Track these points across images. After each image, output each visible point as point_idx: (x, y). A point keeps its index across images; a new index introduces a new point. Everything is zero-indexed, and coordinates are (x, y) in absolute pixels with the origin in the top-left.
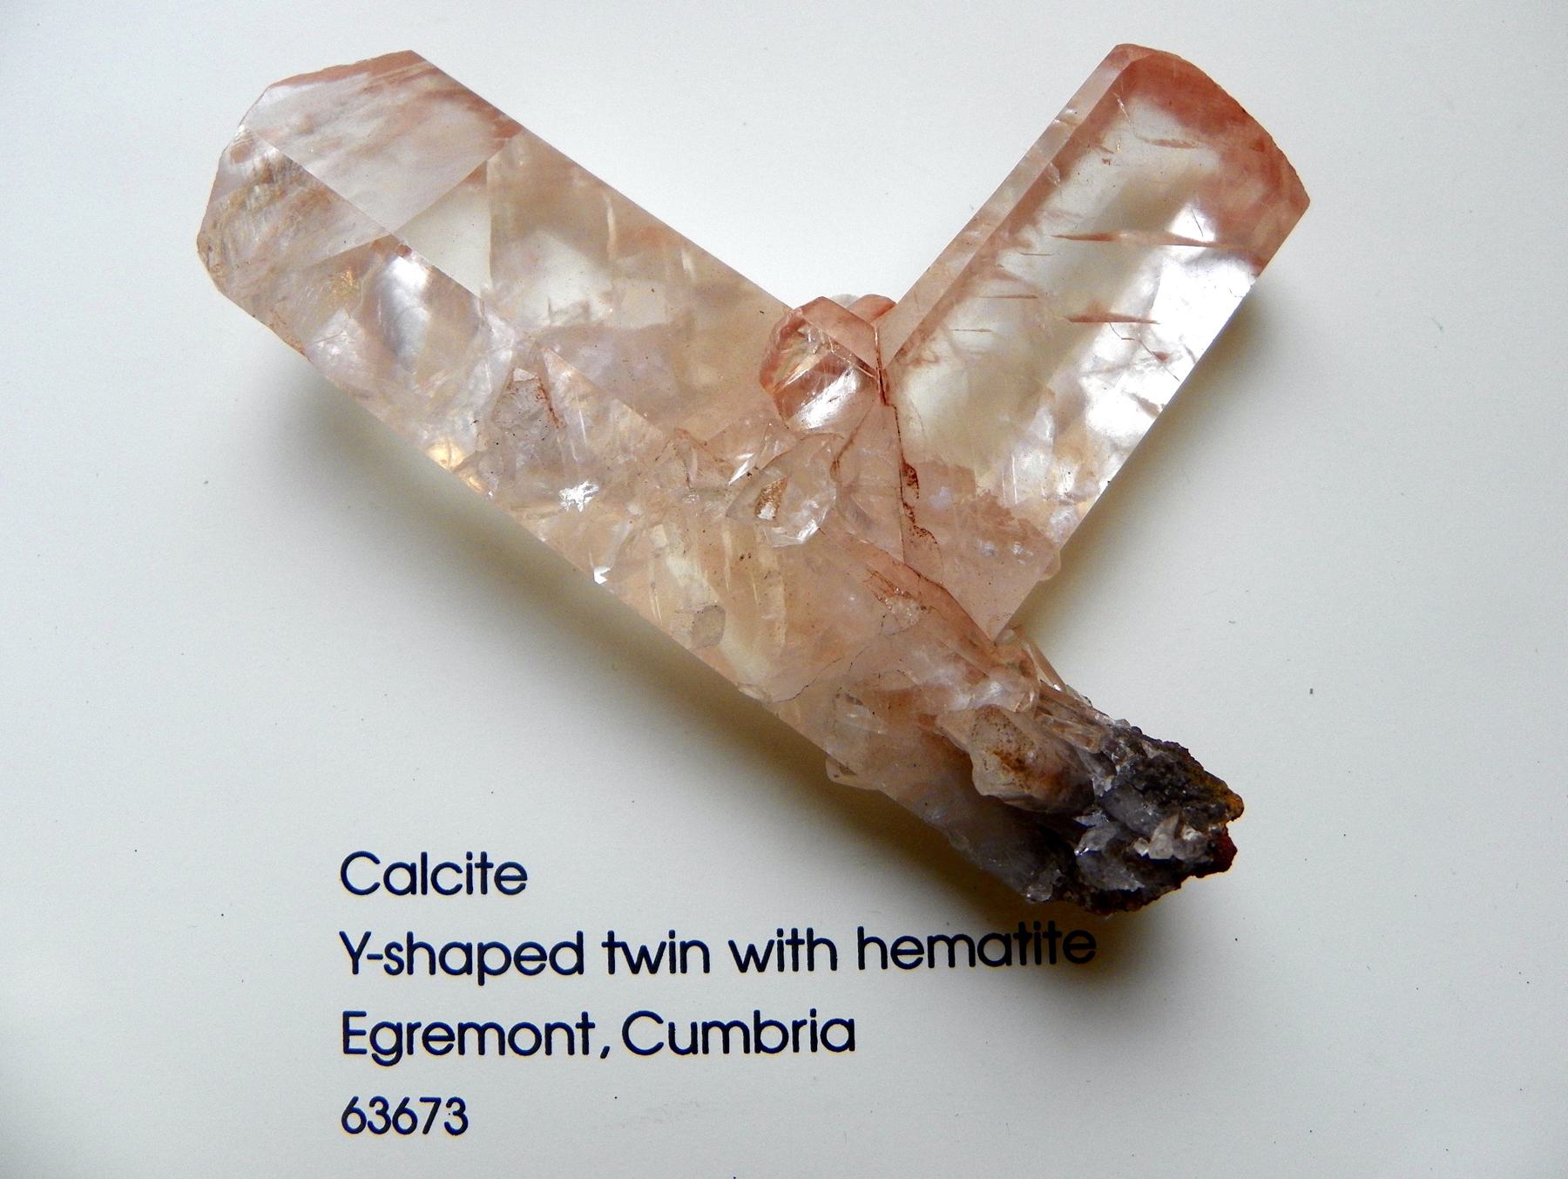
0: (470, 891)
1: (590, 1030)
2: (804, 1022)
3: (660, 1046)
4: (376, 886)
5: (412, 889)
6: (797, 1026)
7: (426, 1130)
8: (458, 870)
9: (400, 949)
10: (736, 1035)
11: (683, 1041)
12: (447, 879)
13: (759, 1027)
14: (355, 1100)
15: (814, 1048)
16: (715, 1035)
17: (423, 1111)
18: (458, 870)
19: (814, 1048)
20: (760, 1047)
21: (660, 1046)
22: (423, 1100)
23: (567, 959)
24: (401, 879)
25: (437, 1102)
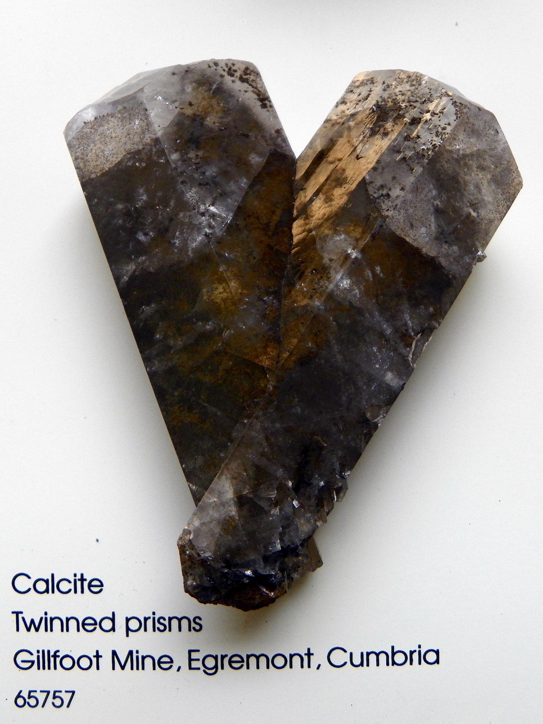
0: (76, 592)
1: (100, 658)
2: (415, 651)
3: (345, 663)
4: (29, 590)
5: (47, 591)
7: (43, 706)
8: (70, 582)
9: (164, 619)
10: (383, 657)
11: (357, 661)
12: (64, 586)
13: (394, 654)
14: (21, 692)
15: (420, 663)
16: (373, 657)
17: (41, 697)
18: (70, 582)
19: (420, 663)
20: (394, 663)
21: (345, 663)
22: (66, 692)
23: (107, 624)
24: (41, 586)
25: (48, 692)
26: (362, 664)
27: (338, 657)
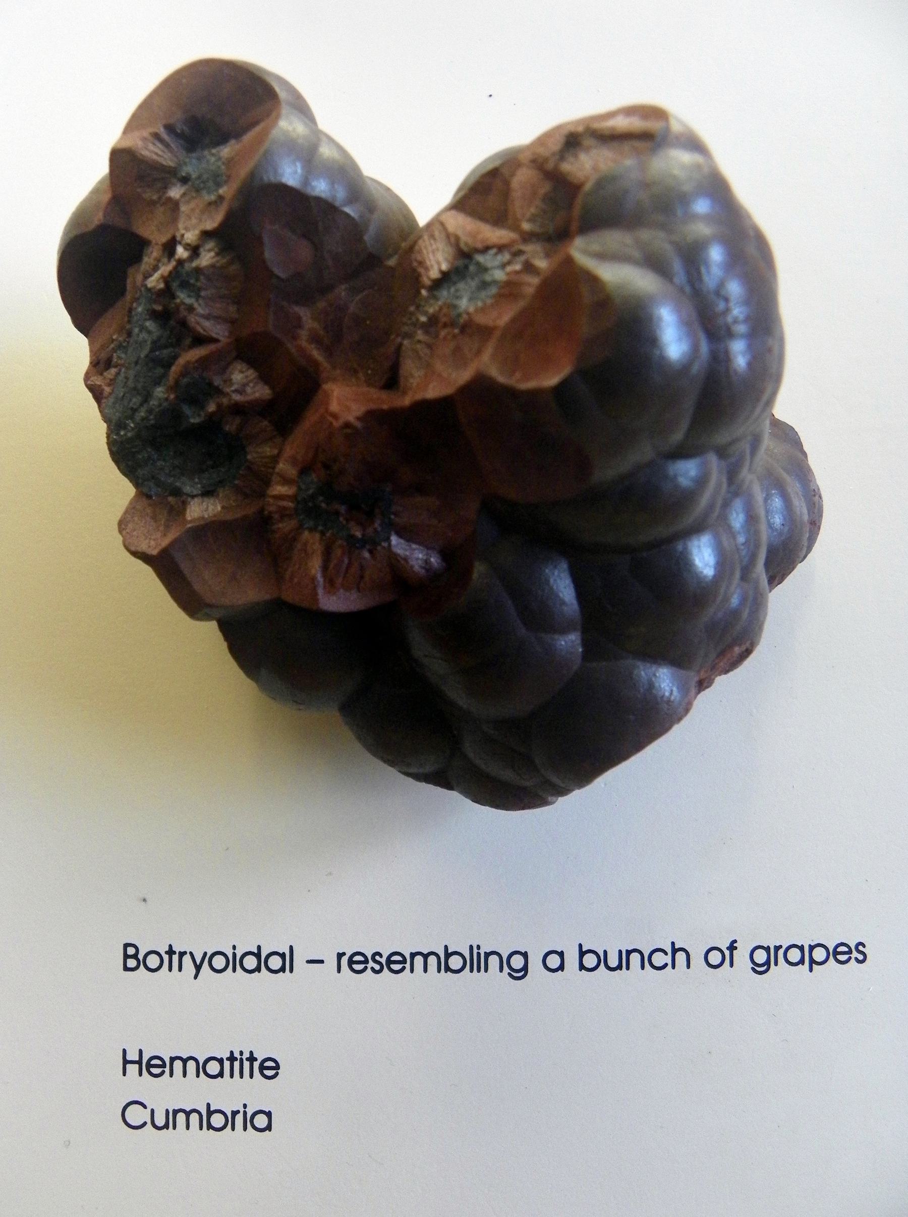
2: (238, 1112)
3: (145, 1124)
6: (235, 1113)
11: (161, 1121)
13: (210, 1113)
15: (245, 1129)
16: (181, 1117)
19: (245, 1129)
21: (145, 1124)
26: (166, 1126)
27: (136, 1115)
